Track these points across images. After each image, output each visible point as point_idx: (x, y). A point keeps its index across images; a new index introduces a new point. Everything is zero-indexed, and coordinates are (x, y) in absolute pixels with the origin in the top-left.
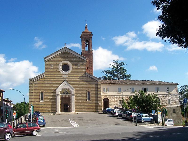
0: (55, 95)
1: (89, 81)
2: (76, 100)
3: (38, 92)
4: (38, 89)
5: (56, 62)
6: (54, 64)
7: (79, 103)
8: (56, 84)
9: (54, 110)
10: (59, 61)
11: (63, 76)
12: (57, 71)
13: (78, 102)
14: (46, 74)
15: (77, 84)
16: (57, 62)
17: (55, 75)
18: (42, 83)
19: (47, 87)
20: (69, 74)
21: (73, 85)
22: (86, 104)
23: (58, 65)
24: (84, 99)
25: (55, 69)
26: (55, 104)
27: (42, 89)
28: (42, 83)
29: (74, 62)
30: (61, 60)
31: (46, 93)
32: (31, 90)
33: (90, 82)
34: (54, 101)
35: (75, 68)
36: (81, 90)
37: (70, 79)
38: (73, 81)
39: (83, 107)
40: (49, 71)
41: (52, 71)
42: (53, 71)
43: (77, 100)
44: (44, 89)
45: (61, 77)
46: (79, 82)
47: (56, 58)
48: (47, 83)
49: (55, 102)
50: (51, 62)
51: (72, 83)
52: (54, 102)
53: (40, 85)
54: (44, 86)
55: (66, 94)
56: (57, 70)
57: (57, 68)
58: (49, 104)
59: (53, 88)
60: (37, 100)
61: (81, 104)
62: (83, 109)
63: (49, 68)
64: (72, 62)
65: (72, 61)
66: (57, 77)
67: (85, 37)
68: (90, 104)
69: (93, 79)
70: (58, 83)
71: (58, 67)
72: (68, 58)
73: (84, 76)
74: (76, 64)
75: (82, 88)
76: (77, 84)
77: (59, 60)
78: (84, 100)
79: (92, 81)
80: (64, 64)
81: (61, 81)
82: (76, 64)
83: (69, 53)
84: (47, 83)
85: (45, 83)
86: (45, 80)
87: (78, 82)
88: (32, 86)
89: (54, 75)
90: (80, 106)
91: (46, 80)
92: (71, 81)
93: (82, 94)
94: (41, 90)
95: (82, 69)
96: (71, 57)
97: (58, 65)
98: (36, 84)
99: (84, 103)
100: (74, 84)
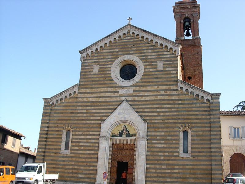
0: (98, 137)
1: (186, 102)
4: (60, 122)
5: (106, 60)
7: (156, 162)
8: (102, 111)
9: (92, 176)
10: (112, 57)
11: (121, 92)
12: (107, 80)
15: (155, 110)
16: (109, 60)
18: (71, 108)
19: (80, 118)
20: (136, 86)
21: (144, 114)
23: (109, 66)
24: (171, 152)
26: (95, 160)
28: (71, 108)
29: (149, 57)
30: (117, 55)
31: (77, 133)
33: (188, 104)
34: (93, 152)
35: (151, 70)
36: (163, 126)
37: (136, 98)
38: (145, 102)
39: (168, 173)
40: (88, 81)
42: (97, 79)
43: (152, 153)
44: (73, 123)
45: (116, 94)
46: (160, 106)
47: (107, 51)
48: (80, 108)
49: (96, 156)
50: (96, 59)
51: (140, 107)
52: (93, 156)
54: (73, 115)
55: (124, 136)
56: (108, 77)
57: (108, 72)
58: (81, 160)
59: (93, 122)
60: (55, 149)
62: (168, 180)
63: (89, 73)
64: (144, 57)
65: (143, 54)
66: (106, 95)
67: (182, 11)
68: (187, 165)
69: (197, 95)
70: (108, 107)
71: (110, 71)
72: (134, 49)
73: (174, 90)
74: (153, 60)
75: (166, 121)
76: (155, 110)
78: (170, 154)
79: (195, 101)
80: (124, 64)
81: (114, 103)
82: (153, 60)
83: (137, 37)
84: (80, 108)
85: (78, 108)
86: (76, 102)
87: (157, 106)
89: (99, 90)
90: (161, 169)
91: (79, 102)
92: (140, 103)
93: (168, 138)
95: (169, 72)
96: (141, 45)
97: (109, 66)
99: (171, 162)
100: (145, 110)
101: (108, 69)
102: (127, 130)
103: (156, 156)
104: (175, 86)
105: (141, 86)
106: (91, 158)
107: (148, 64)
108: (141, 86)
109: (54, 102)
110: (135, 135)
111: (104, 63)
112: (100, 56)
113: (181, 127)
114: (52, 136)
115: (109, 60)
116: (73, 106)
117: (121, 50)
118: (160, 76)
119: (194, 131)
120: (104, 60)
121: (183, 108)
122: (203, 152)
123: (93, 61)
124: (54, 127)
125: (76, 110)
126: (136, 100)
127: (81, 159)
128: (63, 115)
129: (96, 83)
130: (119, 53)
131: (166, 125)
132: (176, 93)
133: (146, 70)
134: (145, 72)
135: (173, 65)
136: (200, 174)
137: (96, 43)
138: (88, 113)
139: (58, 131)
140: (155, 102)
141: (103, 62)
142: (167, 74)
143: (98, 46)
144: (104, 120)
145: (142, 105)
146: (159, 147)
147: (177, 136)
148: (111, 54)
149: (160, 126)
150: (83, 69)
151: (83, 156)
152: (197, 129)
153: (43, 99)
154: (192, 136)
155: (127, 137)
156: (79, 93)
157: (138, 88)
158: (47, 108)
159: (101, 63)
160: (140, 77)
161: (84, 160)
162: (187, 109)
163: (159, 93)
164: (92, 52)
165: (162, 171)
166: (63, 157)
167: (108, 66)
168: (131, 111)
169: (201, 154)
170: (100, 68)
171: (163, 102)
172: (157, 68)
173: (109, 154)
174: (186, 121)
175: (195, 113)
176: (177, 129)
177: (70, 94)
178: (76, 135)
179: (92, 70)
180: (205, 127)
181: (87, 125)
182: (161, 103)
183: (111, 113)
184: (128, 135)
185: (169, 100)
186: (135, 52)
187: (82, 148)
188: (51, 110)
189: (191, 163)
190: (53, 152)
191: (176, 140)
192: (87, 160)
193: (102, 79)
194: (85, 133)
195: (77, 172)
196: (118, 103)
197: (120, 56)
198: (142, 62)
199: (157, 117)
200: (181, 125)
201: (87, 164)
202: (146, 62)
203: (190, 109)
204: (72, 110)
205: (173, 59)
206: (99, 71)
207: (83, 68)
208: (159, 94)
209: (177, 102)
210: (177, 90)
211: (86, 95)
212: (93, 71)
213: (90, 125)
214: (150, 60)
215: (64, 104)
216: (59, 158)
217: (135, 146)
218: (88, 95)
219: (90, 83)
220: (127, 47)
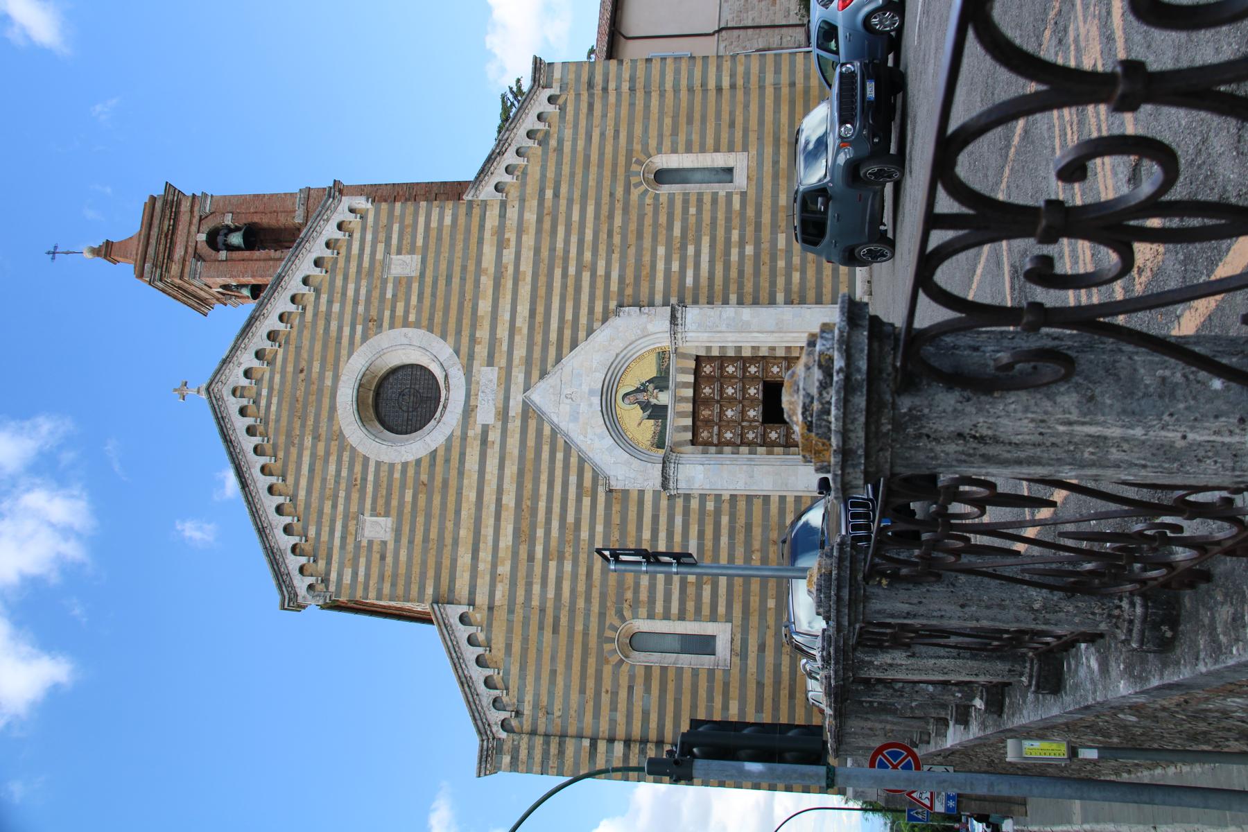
1: (551, 174)
3: (624, 682)
4: (591, 683)
5: (343, 486)
10: (333, 459)
11: (486, 414)
12: (432, 476)
13: (757, 273)
16: (344, 473)
17: (470, 495)
20: (471, 356)
21: (583, 320)
23: (372, 469)
24: (728, 220)
25: (408, 496)
29: (361, 309)
30: (329, 440)
31: (644, 596)
33: (559, 164)
34: (725, 520)
35: (414, 300)
37: (520, 352)
38: (539, 318)
40: (424, 563)
41: (427, 531)
42: (420, 519)
44: (602, 615)
45: (494, 436)
46: (559, 262)
47: (303, 482)
48: (536, 589)
51: (553, 336)
54: (564, 621)
55: (664, 398)
56: (417, 473)
57: (397, 475)
63: (389, 559)
64: (359, 328)
70: (545, 466)
71: (392, 466)
72: (316, 367)
73: (503, 215)
74: (376, 294)
75: (617, 240)
77: (328, 453)
78: (736, 222)
79: (553, 143)
81: (531, 442)
82: (376, 294)
84: (536, 589)
85: (535, 602)
87: (558, 272)
92: (538, 338)
93: (677, 232)
94: (607, 647)
95: (433, 234)
96: (306, 343)
97: (372, 469)
98: (544, 700)
100: (569, 316)
101: (385, 468)
102: (642, 389)
103: (741, 273)
104: (488, 213)
106: (749, 527)
107: (387, 313)
109: (496, 716)
110: (662, 356)
111: (355, 496)
112: (321, 512)
114: (654, 717)
115: (344, 473)
116: (526, 622)
117: (310, 422)
118: (443, 266)
119: (660, 144)
120: (342, 494)
123: (337, 542)
124: (614, 708)
125: (542, 610)
126: (524, 354)
128: (560, 668)
129: (435, 524)
130: (323, 430)
131: (632, 238)
132: (517, 206)
134: (417, 325)
137: (262, 531)
140: (542, 280)
141: (348, 498)
142: (439, 239)
143: (274, 523)
148: (318, 467)
149: (631, 261)
152: (653, 132)
154: (674, 151)
155: (667, 388)
156: (471, 603)
157: (478, 348)
158: (523, 754)
159: (354, 508)
164: (294, 549)
166: (744, 655)
167: (371, 477)
168: (567, 370)
170: (374, 509)
171: (545, 253)
172: (409, 280)
174: (621, 171)
176: (648, 200)
177: (471, 641)
178: (652, 601)
179: (376, 548)
180: (647, 107)
182: (546, 262)
184: (661, 382)
185: (539, 231)
186: (329, 366)
188: (533, 733)
192: (757, 545)
193: (422, 498)
197: (335, 428)
199: (598, 273)
204: (541, 628)
206: (387, 514)
208: (511, 269)
210: (503, 205)
212: (384, 543)
213: (612, 539)
214: (375, 302)
215: (515, 670)
216: (749, 670)
217: (702, 353)
218: (485, 555)
219: (433, 552)
220: (301, 399)
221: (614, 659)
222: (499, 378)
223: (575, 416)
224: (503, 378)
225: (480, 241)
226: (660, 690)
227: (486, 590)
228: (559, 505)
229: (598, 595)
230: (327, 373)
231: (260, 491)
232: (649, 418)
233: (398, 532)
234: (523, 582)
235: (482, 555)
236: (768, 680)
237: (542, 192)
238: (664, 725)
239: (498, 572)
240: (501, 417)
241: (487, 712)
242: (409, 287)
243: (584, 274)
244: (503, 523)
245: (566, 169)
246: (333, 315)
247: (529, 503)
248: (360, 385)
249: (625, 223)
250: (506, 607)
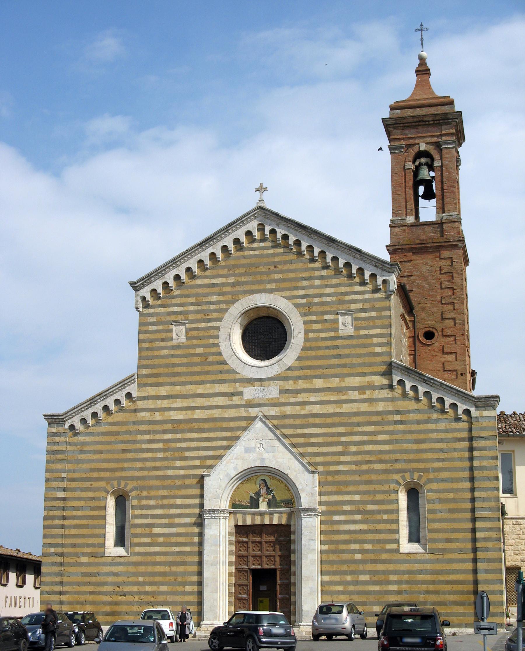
2: (325, 547)
3: (96, 494)
4: (95, 475)
5: (204, 307)
6: (191, 317)
7: (345, 567)
10: (220, 298)
13: (343, 562)
14: (146, 385)
15: (335, 439)
16: (212, 307)
17: (200, 389)
18: (121, 438)
19: (148, 464)
20: (286, 378)
21: (310, 450)
22: (395, 572)
23: (215, 324)
24: (379, 541)
25: (199, 350)
27: (118, 474)
28: (121, 438)
29: (317, 300)
30: (232, 294)
31: (144, 502)
32: (55, 484)
33: (418, 422)
36: (357, 478)
37: (289, 410)
38: (311, 420)
39: (375, 593)
40: (160, 366)
42: (185, 360)
43: (333, 547)
44: (133, 478)
45: (236, 400)
46: (349, 429)
47: (206, 281)
48: (147, 437)
51: (300, 431)
53: (109, 451)
54: (129, 455)
55: (263, 507)
56: (213, 354)
57: (211, 341)
58: (158, 569)
59: (182, 472)
60: (89, 545)
61: (364, 573)
63: (162, 344)
64: (304, 301)
65: (302, 292)
68: (420, 572)
71: (217, 337)
72: (279, 276)
73: (382, 387)
74: (327, 308)
75: (365, 467)
76: (335, 439)
78: (378, 547)
80: (253, 315)
81: (232, 424)
84: (147, 437)
85: (140, 437)
87: (341, 430)
88: (60, 456)
90: (357, 583)
92: (298, 422)
93: (370, 507)
94: (115, 483)
95: (368, 341)
97: (215, 324)
98: (86, 448)
99: (380, 567)
100: (313, 440)
101: (213, 332)
103: (343, 552)
105: (300, 378)
107: (314, 318)
108: (300, 378)
109: (76, 421)
111: (198, 316)
112: (187, 296)
113: (401, 481)
115: (212, 307)
116: (129, 432)
117: (243, 279)
118: (346, 351)
120: (200, 308)
121: (404, 432)
122: (457, 540)
123: (171, 309)
125: (135, 442)
127: (158, 567)
128: (104, 456)
130: (239, 288)
131: (365, 477)
132: (389, 396)
133: (311, 335)
134: (307, 340)
135: (378, 322)
136: (450, 593)
138: (167, 452)
139: (93, 498)
140: (337, 420)
141: (197, 312)
143: (180, 268)
144: (211, 467)
145: (302, 426)
146: (350, 532)
147: (391, 502)
148: (216, 289)
149: (350, 478)
150: (146, 332)
151: (163, 559)
153: (45, 416)
155: (269, 507)
157: (291, 382)
160: (294, 353)
161: (167, 569)
162: (414, 436)
163: (345, 395)
165: (361, 588)
167: (210, 324)
169: (453, 546)
170: (191, 329)
171: (356, 419)
172: (337, 329)
173: (230, 552)
174: (415, 466)
175: (436, 444)
176: (393, 486)
179: (169, 334)
181: (169, 482)
182: (349, 421)
183: (228, 448)
187: (161, 540)
189: (428, 567)
190: (84, 555)
191: (391, 512)
193: (198, 359)
194: (166, 502)
195: (152, 599)
196: (243, 424)
197: (240, 296)
198: (298, 315)
199: (341, 457)
200: (400, 475)
201: (175, 580)
202: (310, 315)
203: (422, 436)
205: (378, 306)
206: (188, 338)
207: (145, 328)
208: (344, 397)
209: (391, 418)
211: (159, 402)
212: (171, 339)
213: (176, 480)
216: (104, 567)
218: (164, 403)
220: (258, 270)
221: (109, 488)
222: (272, 399)
223: (248, 450)
224: (272, 402)
225: (364, 374)
226: (93, 516)
227: (146, 407)
228: (195, 446)
229: (144, 475)
230: (274, 284)
231: (199, 255)
232: (251, 497)
233: (178, 347)
234: (150, 429)
235: (165, 401)
236: (99, 579)
237: (399, 412)
238: (74, 519)
239: (156, 413)
240: (248, 403)
241: (78, 416)
242: (332, 330)
243: (341, 447)
244: (184, 412)
245: (414, 427)
246: (312, 281)
247: (196, 427)
248: (268, 307)
249: (377, 472)
250: (136, 420)
